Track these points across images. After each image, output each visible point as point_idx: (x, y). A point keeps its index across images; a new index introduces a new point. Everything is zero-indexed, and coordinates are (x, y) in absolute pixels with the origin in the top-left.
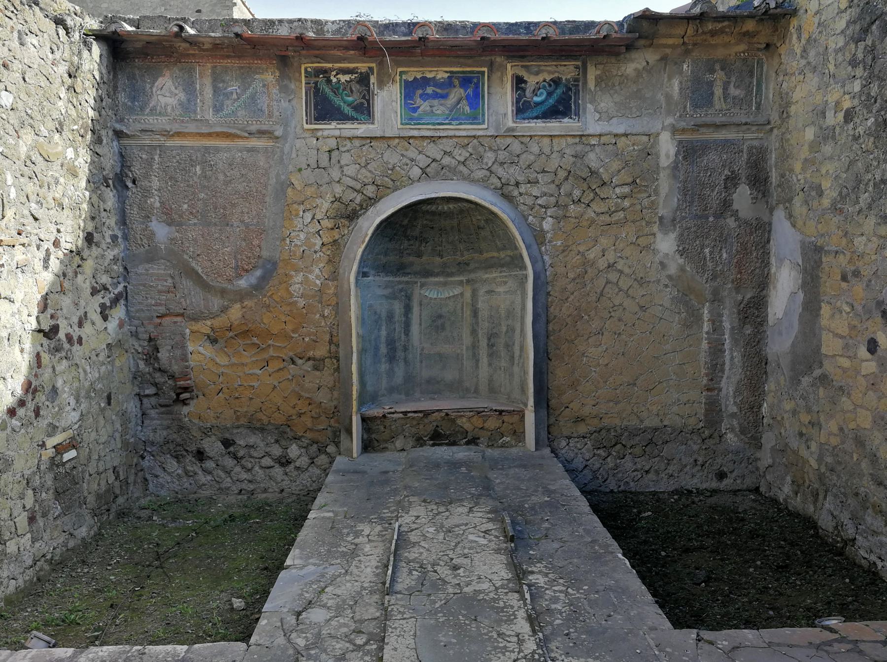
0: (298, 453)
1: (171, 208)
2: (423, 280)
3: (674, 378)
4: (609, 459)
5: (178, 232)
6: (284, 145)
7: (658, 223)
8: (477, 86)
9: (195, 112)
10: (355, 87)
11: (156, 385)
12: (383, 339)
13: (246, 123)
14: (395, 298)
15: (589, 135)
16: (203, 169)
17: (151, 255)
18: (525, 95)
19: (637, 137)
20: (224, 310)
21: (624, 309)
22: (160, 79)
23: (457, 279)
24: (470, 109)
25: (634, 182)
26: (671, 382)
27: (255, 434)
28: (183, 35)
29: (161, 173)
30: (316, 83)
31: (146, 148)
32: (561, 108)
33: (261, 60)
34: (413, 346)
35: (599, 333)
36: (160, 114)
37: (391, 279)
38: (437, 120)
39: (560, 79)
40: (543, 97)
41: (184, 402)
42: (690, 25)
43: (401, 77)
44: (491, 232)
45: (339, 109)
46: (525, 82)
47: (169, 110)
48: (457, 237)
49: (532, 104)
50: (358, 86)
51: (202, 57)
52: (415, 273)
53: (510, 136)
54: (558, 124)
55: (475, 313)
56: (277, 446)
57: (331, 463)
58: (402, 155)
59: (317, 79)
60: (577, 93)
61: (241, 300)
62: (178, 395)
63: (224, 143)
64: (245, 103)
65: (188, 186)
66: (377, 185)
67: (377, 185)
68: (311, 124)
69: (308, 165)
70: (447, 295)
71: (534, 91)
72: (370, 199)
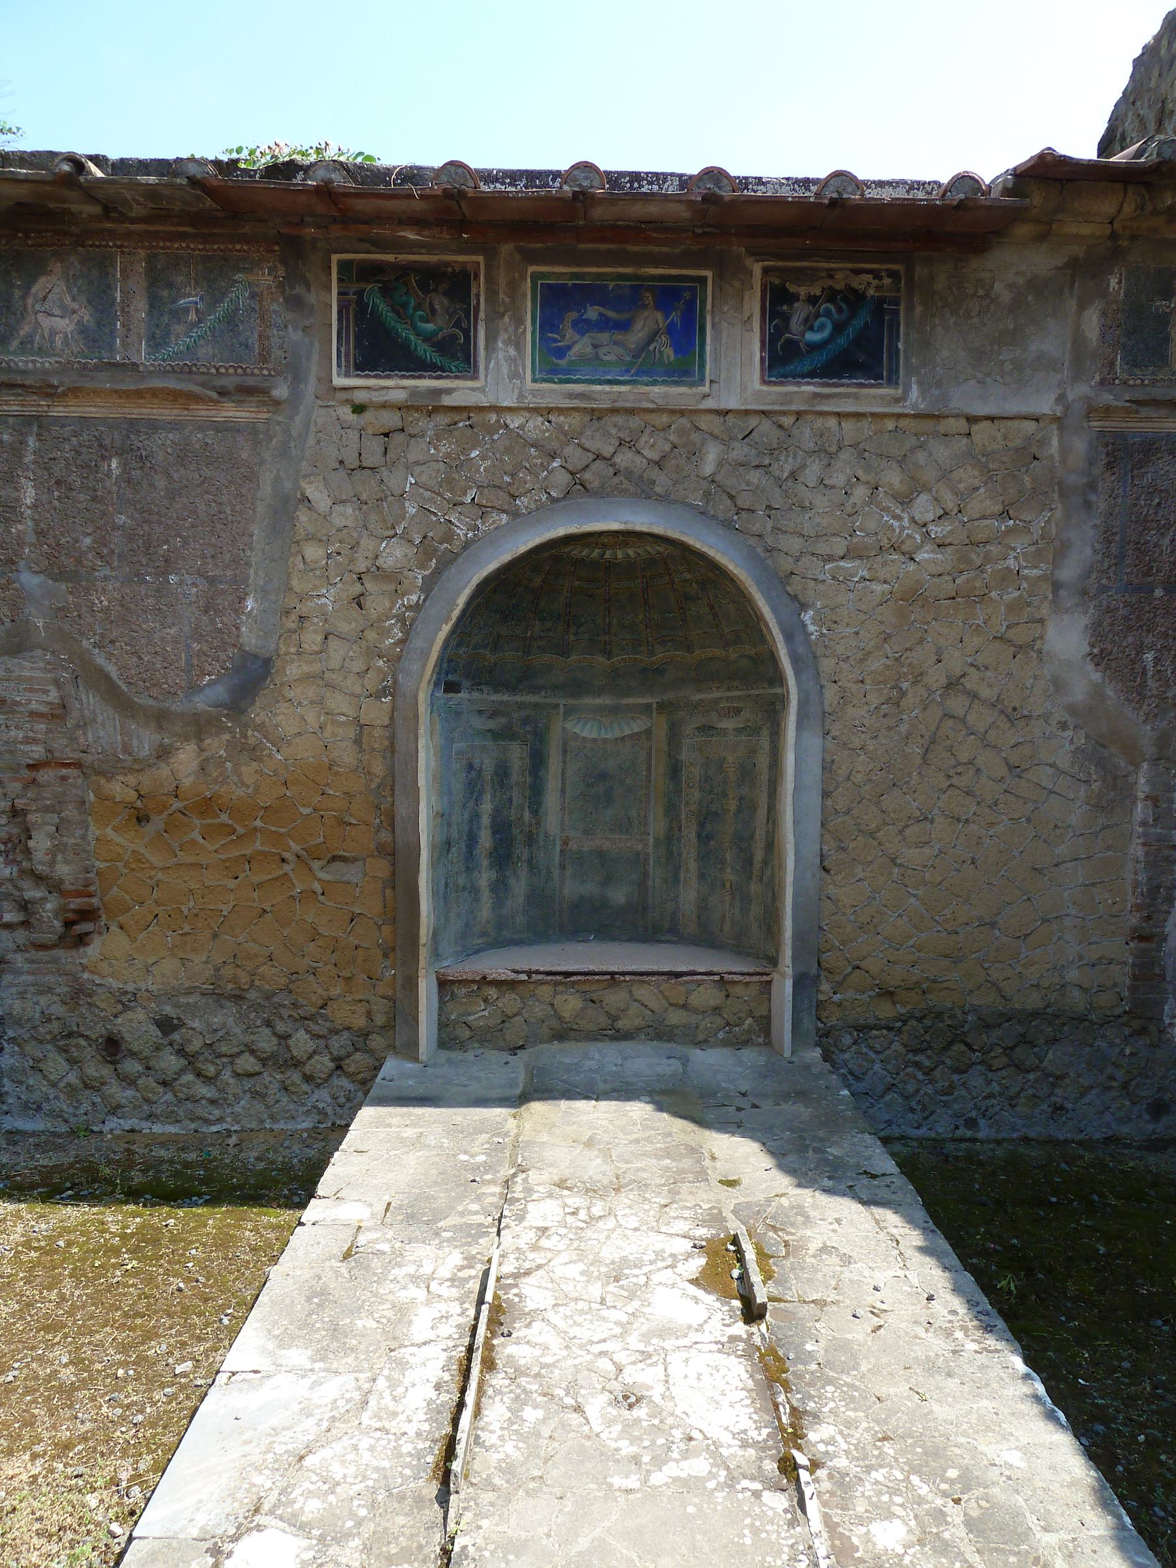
0: (311, 1045)
1: (58, 545)
2: (570, 701)
3: (1073, 911)
4: (937, 1074)
5: (71, 593)
6: (291, 418)
7: (1050, 596)
8: (690, 306)
9: (111, 348)
10: (440, 302)
11: (25, 906)
12: (486, 821)
13: (213, 371)
14: (513, 737)
16: (124, 465)
17: (17, 640)
18: (787, 329)
19: (1009, 423)
20: (163, 753)
21: (978, 770)
22: (42, 280)
23: (640, 701)
24: (676, 353)
25: (1005, 514)
26: (1068, 922)
27: (223, 1008)
28: (82, 179)
29: (40, 472)
30: (360, 293)
31: (11, 420)
33: (248, 242)
34: (547, 836)
35: (926, 819)
36: (41, 352)
37: (505, 698)
38: (608, 373)
40: (826, 333)
41: (81, 940)
42: (1130, 195)
44: (712, 607)
45: (405, 347)
47: (59, 341)
48: (641, 616)
50: (446, 301)
51: (129, 235)
52: (556, 688)
55: (675, 770)
56: (267, 1031)
57: (377, 1069)
59: (363, 285)
60: (894, 326)
61: (200, 740)
62: (68, 924)
63: (167, 412)
64: (212, 329)
65: (94, 499)
68: (347, 375)
69: (341, 462)
70: (618, 734)
71: (806, 320)
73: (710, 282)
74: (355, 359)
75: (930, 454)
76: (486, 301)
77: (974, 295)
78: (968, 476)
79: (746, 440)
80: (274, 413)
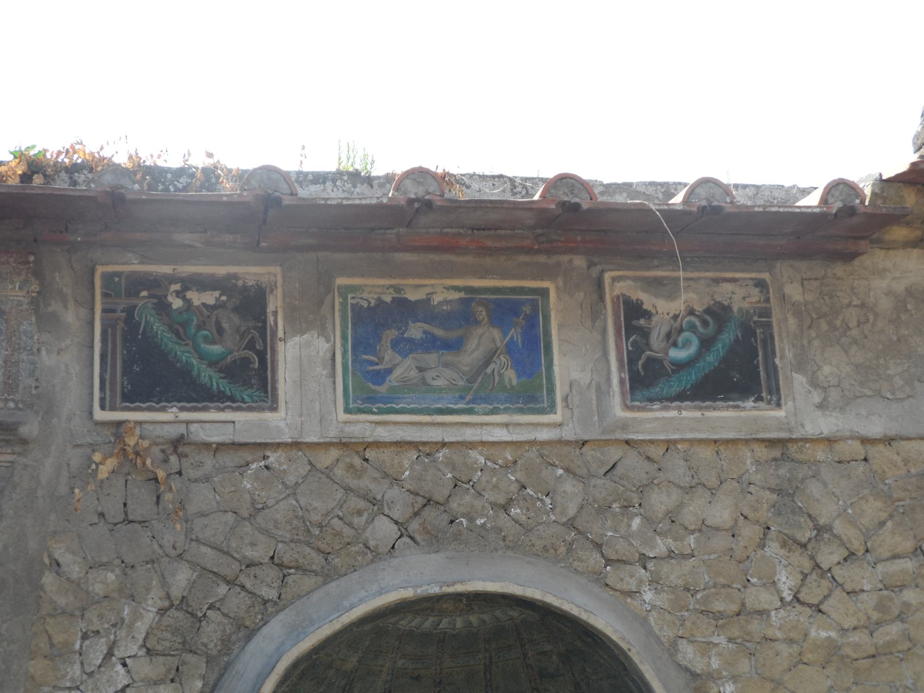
10: (230, 322)
15: (806, 440)
18: (648, 345)
24: (519, 376)
30: (130, 311)
32: (736, 377)
39: (727, 309)
40: (692, 350)
43: (345, 299)
46: (647, 315)
49: (667, 364)
50: (236, 319)
53: (617, 441)
54: (731, 413)
58: (348, 489)
59: (134, 301)
60: (769, 340)
66: (281, 566)
67: (281, 566)
68: (113, 408)
69: (102, 515)
71: (668, 335)
72: (265, 602)
73: (553, 294)
74: (123, 387)
75: (825, 485)
76: (285, 318)
77: (849, 305)
78: (873, 509)
79: (609, 475)
80: (20, 454)
